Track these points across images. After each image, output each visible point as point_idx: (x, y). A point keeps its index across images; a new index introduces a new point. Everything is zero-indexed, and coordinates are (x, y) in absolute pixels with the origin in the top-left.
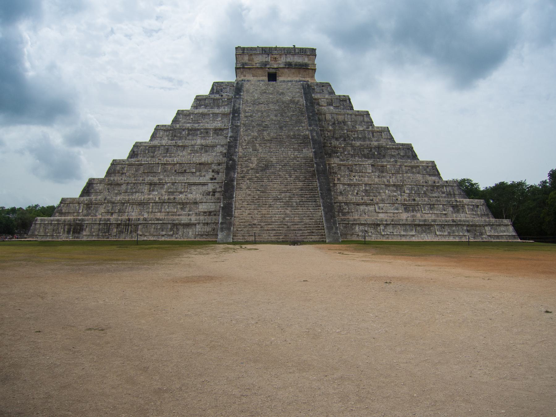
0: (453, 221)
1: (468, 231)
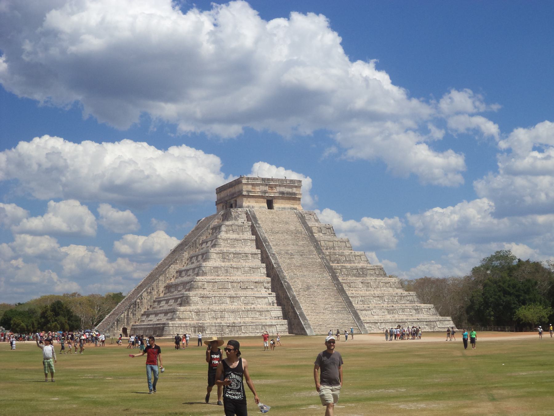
0: (418, 319)
1: (427, 325)
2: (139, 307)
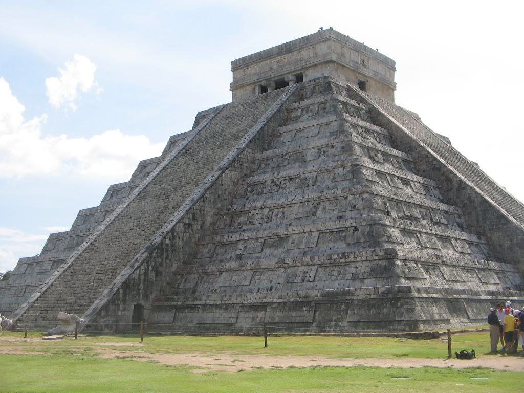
2: (167, 258)
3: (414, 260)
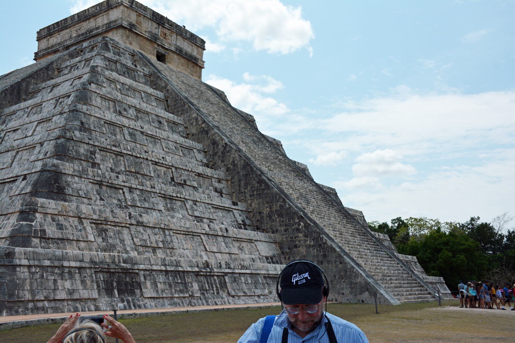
3: (77, 216)
